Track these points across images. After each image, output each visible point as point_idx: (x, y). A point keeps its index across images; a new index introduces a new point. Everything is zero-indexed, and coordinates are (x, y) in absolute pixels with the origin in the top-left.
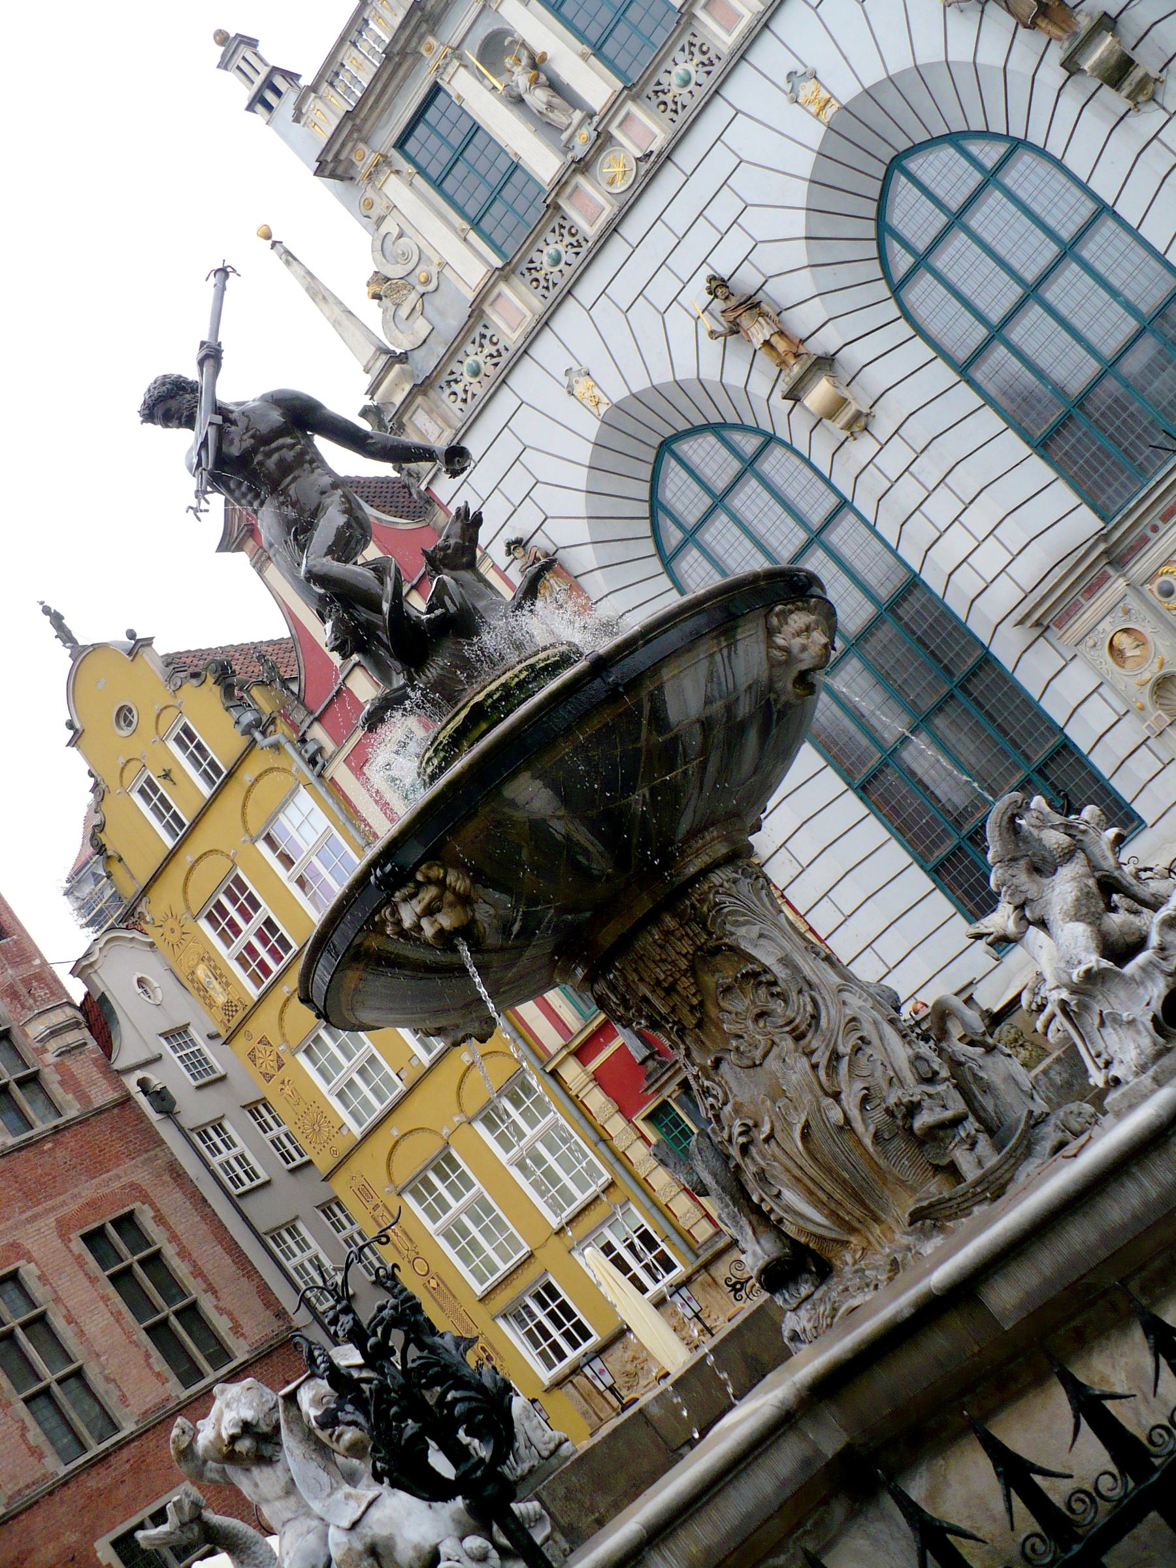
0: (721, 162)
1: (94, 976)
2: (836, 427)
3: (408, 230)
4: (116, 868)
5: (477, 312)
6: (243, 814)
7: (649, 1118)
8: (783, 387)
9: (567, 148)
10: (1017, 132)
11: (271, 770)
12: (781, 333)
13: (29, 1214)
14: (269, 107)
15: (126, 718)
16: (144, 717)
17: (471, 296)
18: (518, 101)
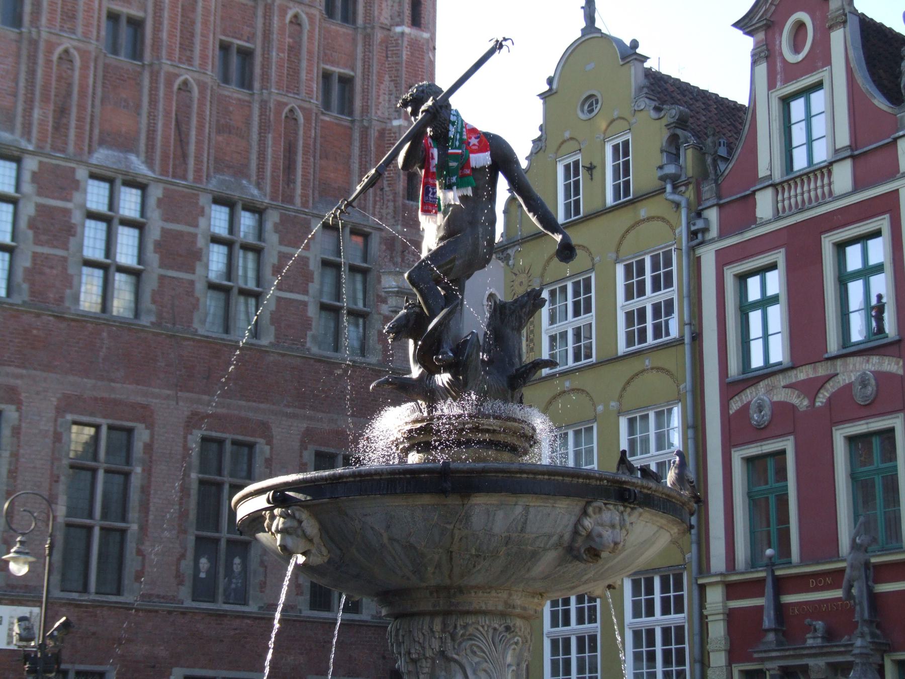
6: (623, 237)
11: (663, 219)
13: (289, 410)
15: (591, 105)
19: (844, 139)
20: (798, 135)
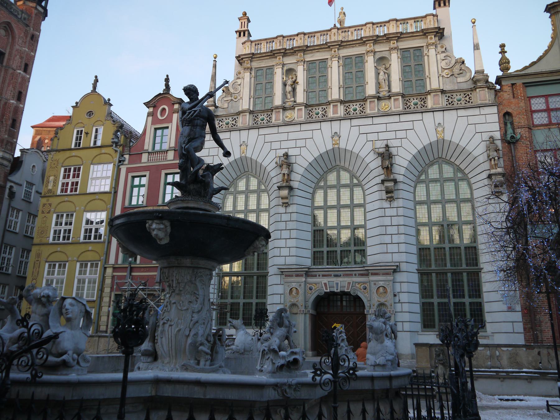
0: (308, 134)
1: (24, 156)
2: (281, 201)
3: (242, 84)
4: (56, 140)
5: (239, 113)
7: (116, 295)
8: (279, 184)
9: (284, 103)
10: (363, 183)
11: (110, 155)
12: (288, 175)
14: (240, 36)
16: (94, 118)
17: (240, 110)
18: (285, 85)
19: (173, 145)
20: (158, 140)
